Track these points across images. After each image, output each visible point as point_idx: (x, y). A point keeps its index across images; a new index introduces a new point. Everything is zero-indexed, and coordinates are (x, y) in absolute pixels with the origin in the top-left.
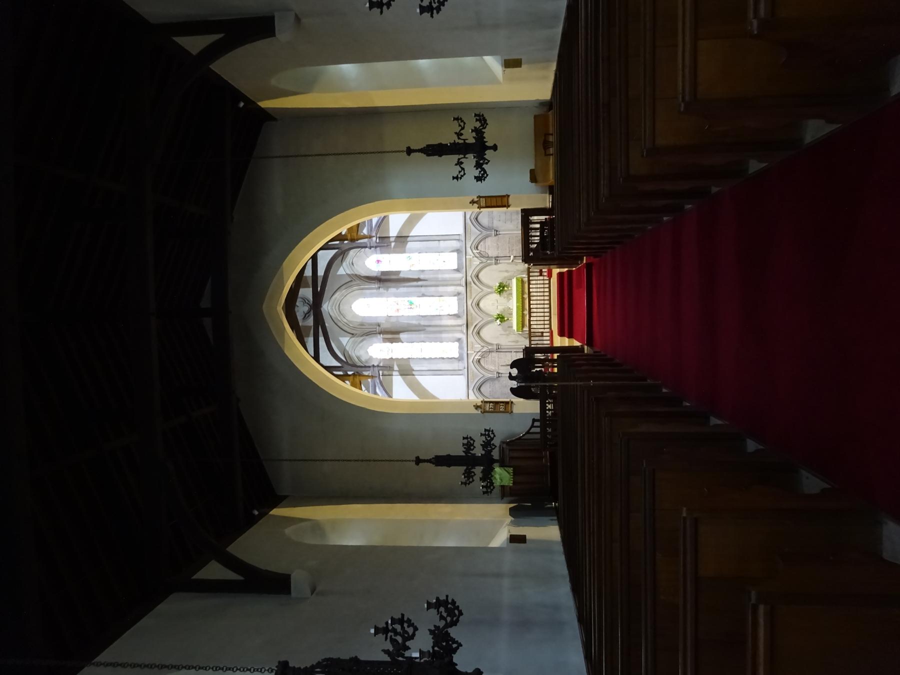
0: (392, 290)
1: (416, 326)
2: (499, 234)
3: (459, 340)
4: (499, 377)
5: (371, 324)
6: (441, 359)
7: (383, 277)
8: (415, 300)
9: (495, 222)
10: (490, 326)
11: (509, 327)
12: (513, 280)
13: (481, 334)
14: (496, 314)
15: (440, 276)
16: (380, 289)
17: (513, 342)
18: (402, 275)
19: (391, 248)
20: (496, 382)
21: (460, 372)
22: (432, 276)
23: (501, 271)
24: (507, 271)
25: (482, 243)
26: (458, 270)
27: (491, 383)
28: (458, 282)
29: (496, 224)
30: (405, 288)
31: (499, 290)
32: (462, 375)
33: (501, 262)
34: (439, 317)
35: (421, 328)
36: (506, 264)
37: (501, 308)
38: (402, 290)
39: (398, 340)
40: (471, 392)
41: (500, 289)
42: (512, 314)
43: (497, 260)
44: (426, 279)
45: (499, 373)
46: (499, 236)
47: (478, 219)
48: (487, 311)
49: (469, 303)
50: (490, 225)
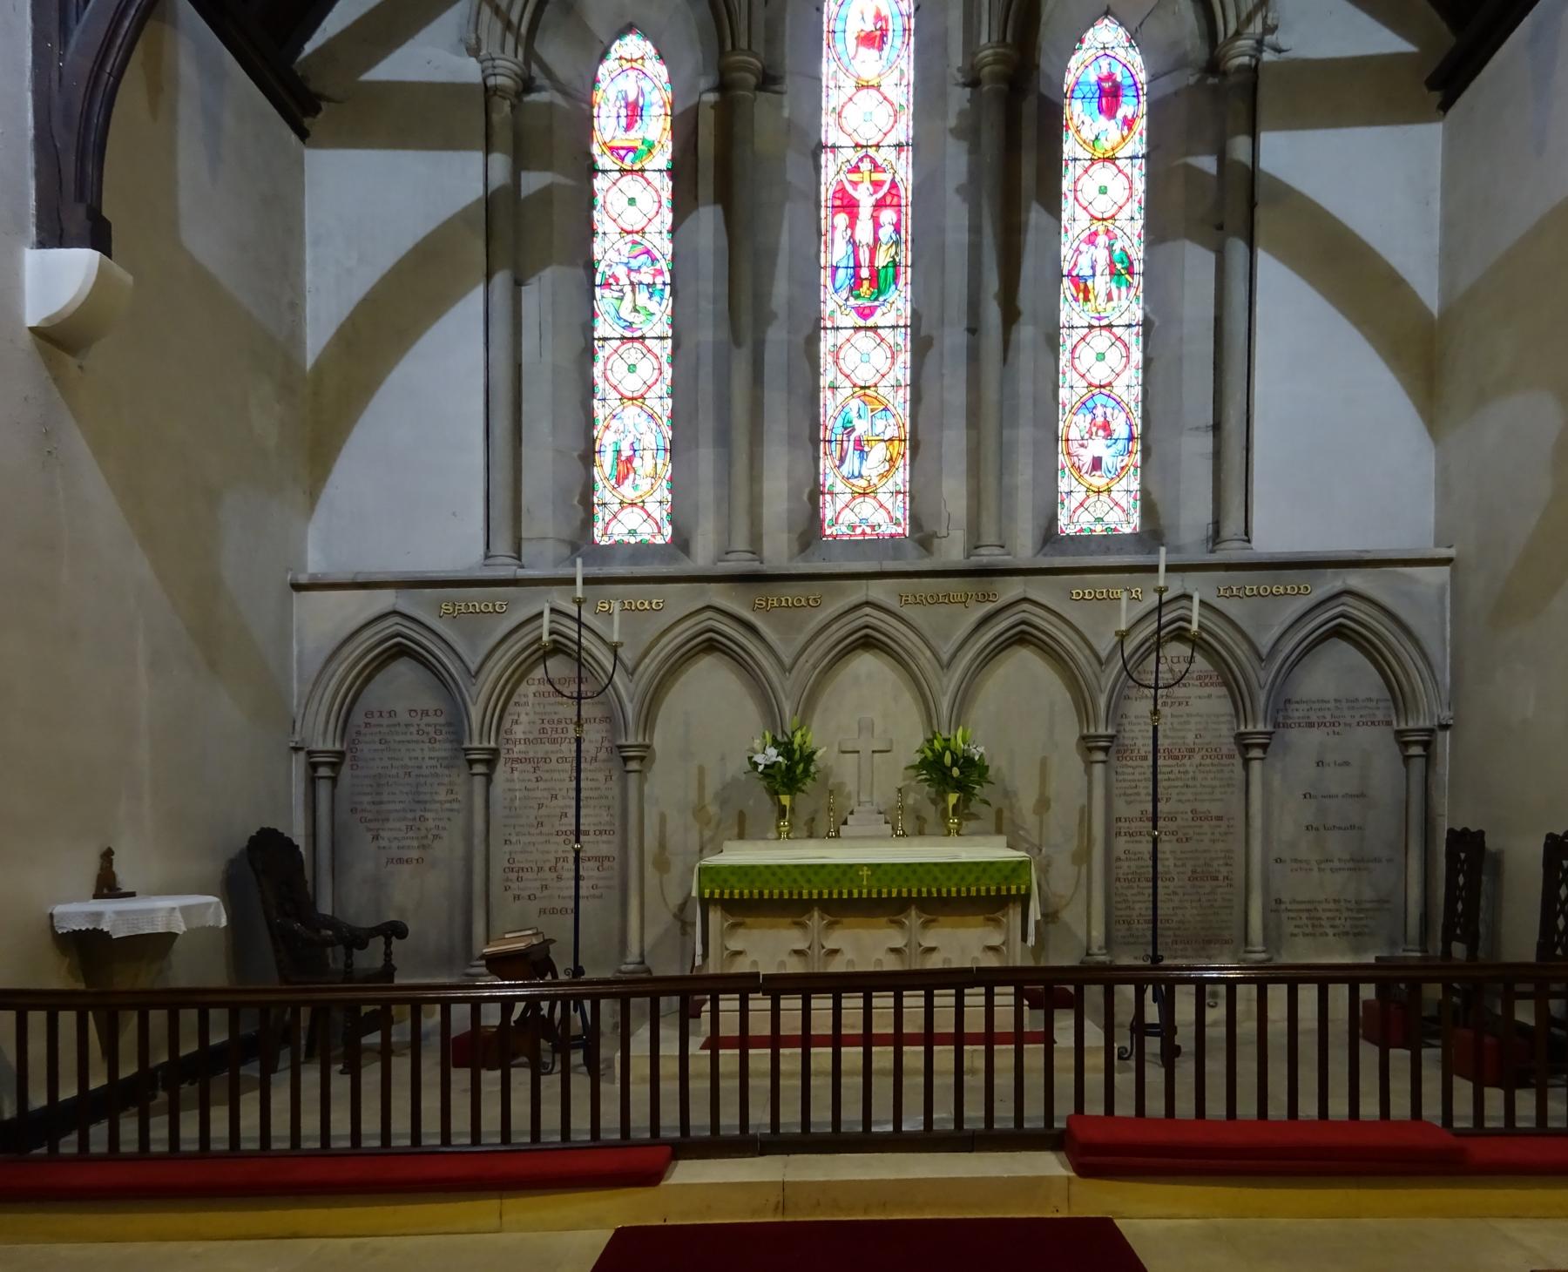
0: (956, 161)
1: (761, 298)
2: (1246, 763)
3: (681, 542)
4: (471, 763)
5: (773, 36)
6: (581, 446)
7: (1029, 107)
8: (897, 305)
9: (1316, 736)
10: (751, 709)
11: (742, 818)
12: (1003, 839)
13: (707, 663)
14: (812, 740)
15: (1024, 434)
16: (968, 90)
17: (662, 845)
18: (1035, 216)
19: (1189, 153)
20: (442, 749)
21: (502, 545)
22: (1025, 387)
23: (1044, 764)
24: (1043, 804)
25: (1201, 663)
26: (1049, 535)
27: (442, 720)
28: (989, 536)
29: (1305, 741)
30: (964, 237)
31: (948, 759)
32: (487, 557)
33: (1098, 770)
34: (806, 433)
35: (746, 319)
36: (1084, 801)
37: (846, 771)
38: (956, 217)
39: (683, 204)
40: (385, 600)
41: (955, 763)
42: (811, 836)
43: (1106, 750)
44: (1011, 354)
45: (491, 764)
46: (1238, 761)
47: (1335, 640)
48: (826, 699)
49: (877, 591)
50: (1297, 713)
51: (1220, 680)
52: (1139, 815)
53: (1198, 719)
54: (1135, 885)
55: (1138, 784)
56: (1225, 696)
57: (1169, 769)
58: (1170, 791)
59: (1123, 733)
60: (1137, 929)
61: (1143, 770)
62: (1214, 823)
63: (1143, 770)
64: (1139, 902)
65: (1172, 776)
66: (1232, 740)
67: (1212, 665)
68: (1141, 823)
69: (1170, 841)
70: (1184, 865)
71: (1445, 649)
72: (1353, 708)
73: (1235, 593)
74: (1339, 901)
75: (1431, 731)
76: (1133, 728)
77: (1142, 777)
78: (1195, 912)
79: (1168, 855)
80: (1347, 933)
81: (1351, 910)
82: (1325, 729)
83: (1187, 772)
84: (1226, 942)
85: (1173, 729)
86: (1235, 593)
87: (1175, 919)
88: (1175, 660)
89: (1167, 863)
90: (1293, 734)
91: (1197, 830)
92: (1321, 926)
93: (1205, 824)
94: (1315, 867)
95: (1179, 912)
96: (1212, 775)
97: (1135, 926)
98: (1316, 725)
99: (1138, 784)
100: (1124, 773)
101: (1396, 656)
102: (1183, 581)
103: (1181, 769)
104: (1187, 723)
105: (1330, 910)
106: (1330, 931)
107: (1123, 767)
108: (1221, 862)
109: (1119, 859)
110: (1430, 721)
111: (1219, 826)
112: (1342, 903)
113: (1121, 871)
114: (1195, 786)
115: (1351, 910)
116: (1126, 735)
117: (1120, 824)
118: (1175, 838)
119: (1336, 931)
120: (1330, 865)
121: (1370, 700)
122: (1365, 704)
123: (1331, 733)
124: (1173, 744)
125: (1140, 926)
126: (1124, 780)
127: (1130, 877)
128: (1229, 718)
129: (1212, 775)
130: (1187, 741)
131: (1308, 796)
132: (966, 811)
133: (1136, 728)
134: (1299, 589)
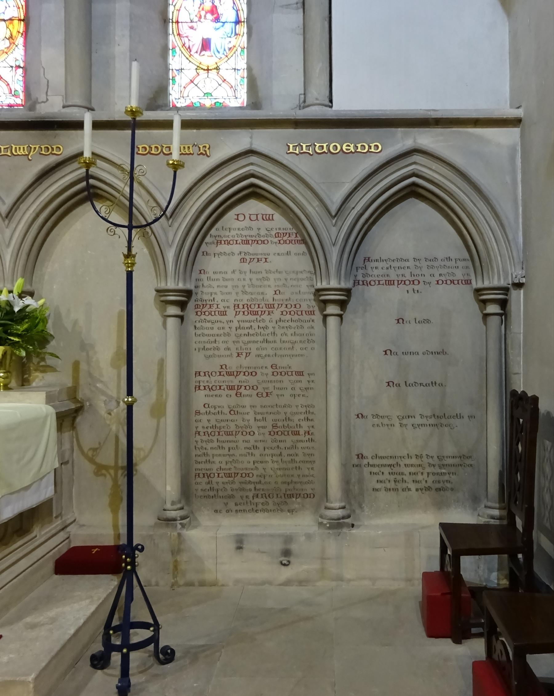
2: (325, 317)
46: (318, 317)
51: (299, 238)
52: (218, 369)
53: (277, 276)
54: (215, 438)
55: (218, 339)
57: (248, 325)
58: (250, 345)
59: (201, 289)
60: (217, 483)
61: (221, 325)
62: (294, 378)
63: (221, 325)
64: (220, 455)
65: (251, 332)
66: (312, 297)
67: (292, 226)
68: (221, 378)
69: (251, 396)
70: (264, 419)
71: (517, 209)
72: (432, 267)
73: (304, 150)
74: (421, 457)
75: (506, 290)
76: (211, 282)
77: (222, 332)
78: (276, 466)
79: (248, 409)
80: (429, 489)
81: (434, 466)
82: (406, 288)
83: (266, 327)
85: (253, 286)
86: (304, 150)
87: (255, 473)
88: (253, 217)
89: (247, 417)
90: (373, 291)
91: (278, 385)
92: (403, 481)
93: (286, 378)
94: (397, 423)
95: (259, 466)
96: (292, 331)
97: (215, 479)
98: (396, 283)
99: (218, 339)
100: (202, 328)
101: (469, 216)
102: (251, 138)
103: (262, 325)
104: (268, 279)
105: (412, 465)
106: (413, 486)
107: (201, 321)
108: (302, 417)
109: (198, 413)
110: (505, 280)
111: (300, 381)
113: (200, 425)
114: (275, 342)
115: (434, 466)
116: (205, 290)
117: (199, 378)
118: (255, 392)
119: (419, 486)
120: (411, 421)
121: (449, 259)
122: (443, 263)
123: (411, 292)
124: (252, 300)
125: (220, 480)
126: (203, 335)
127: (210, 430)
128: (309, 275)
129: (292, 331)
130: (266, 297)
131: (388, 352)
132: (42, 363)
133: (215, 284)
134: (370, 147)
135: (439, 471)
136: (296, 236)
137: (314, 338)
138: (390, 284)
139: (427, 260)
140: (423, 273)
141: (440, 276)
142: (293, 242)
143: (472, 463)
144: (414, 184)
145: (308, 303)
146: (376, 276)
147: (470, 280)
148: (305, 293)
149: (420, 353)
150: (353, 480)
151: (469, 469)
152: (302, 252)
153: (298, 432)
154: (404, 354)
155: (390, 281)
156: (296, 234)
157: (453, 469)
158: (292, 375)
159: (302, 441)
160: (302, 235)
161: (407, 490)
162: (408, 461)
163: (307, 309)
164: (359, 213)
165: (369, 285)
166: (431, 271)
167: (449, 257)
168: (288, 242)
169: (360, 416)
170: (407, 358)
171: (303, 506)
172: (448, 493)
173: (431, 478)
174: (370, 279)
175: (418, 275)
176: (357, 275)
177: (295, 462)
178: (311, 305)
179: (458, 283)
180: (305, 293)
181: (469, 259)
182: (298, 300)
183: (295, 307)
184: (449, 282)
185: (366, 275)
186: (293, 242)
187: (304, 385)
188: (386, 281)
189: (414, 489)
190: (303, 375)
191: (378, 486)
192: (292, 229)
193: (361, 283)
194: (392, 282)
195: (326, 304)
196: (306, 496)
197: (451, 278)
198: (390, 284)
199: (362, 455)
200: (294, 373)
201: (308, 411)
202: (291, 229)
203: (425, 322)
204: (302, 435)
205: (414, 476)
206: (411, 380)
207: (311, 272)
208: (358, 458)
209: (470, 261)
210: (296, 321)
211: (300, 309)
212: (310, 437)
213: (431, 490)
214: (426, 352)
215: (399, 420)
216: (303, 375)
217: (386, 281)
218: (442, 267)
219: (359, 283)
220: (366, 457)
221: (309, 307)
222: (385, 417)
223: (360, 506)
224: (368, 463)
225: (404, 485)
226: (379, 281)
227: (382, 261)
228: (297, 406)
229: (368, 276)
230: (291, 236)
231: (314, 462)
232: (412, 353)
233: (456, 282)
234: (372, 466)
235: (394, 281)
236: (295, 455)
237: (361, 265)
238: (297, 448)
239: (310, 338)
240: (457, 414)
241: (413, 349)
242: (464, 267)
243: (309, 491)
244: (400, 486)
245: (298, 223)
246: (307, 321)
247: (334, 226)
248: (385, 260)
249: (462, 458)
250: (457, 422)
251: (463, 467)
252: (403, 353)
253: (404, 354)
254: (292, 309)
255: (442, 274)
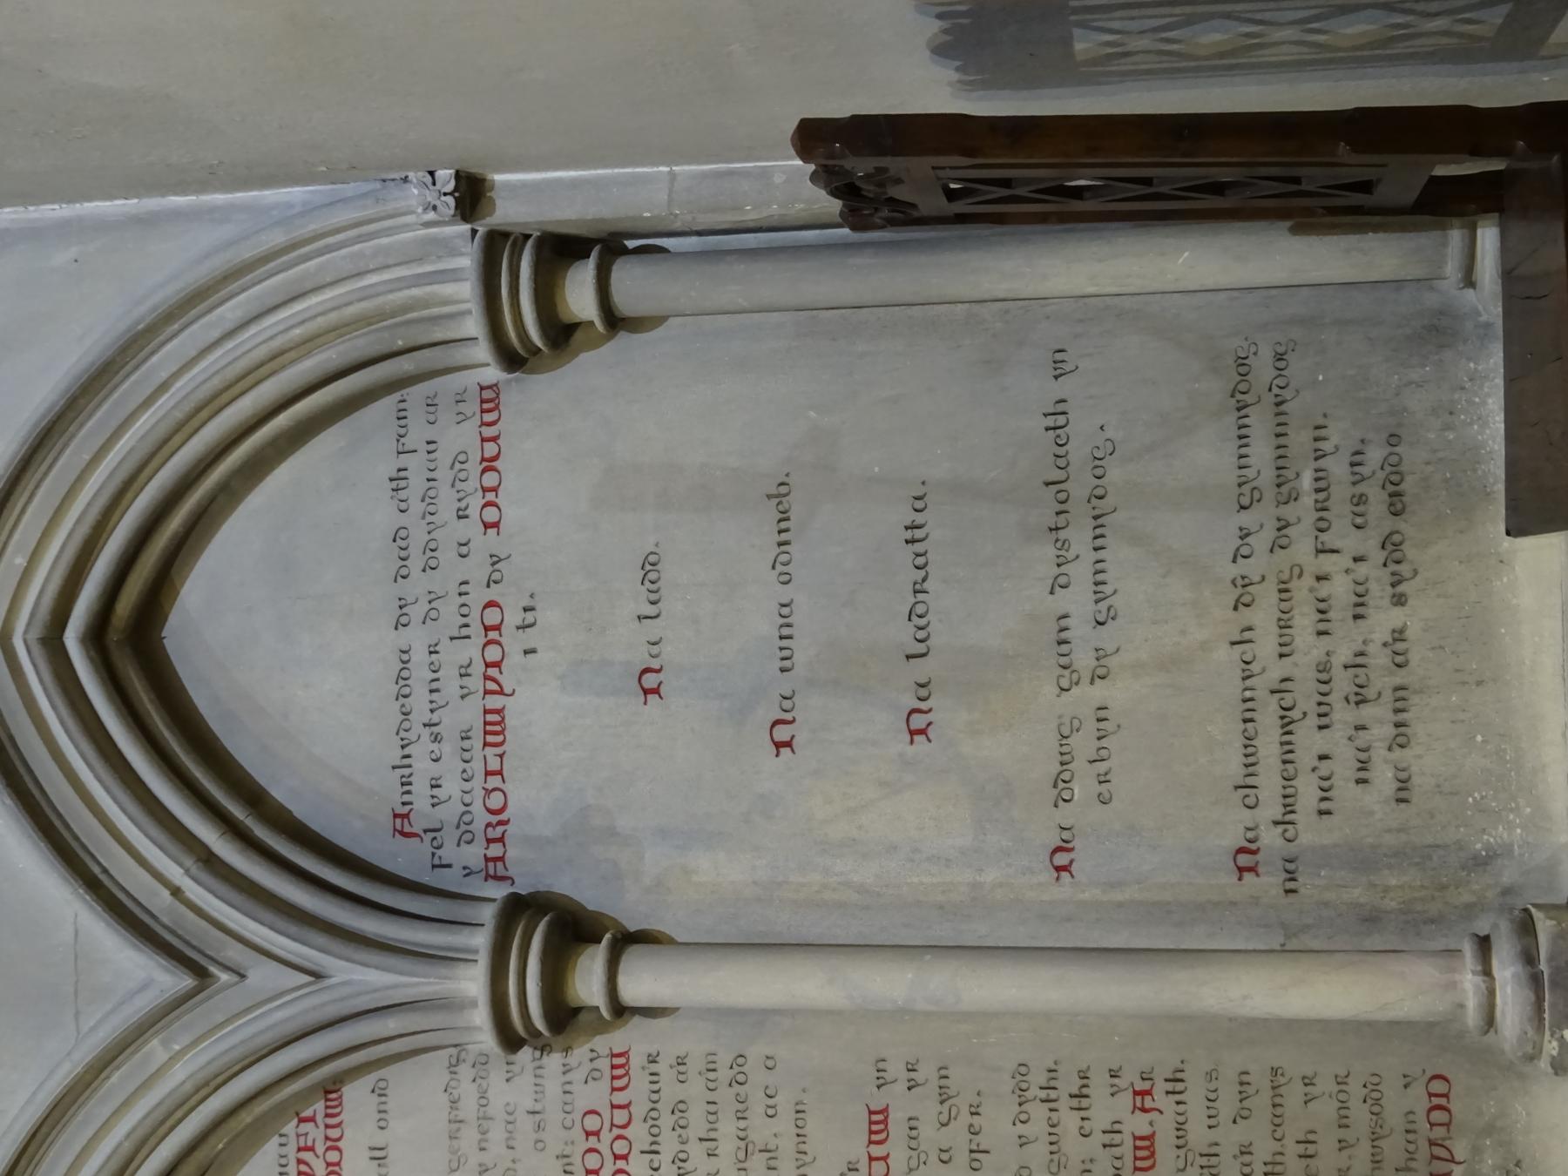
46: (633, 1038)
51: (319, 1107)
56: (380, 1092)
66: (554, 1061)
72: (431, 549)
82: (514, 658)
84: (1439, 1104)
96: (696, 1151)
98: (494, 702)
105: (1284, 625)
108: (1070, 1121)
111: (912, 1125)
112: (1252, 568)
119: (1379, 592)
120: (1079, 629)
121: (398, 479)
122: (417, 507)
123: (530, 638)
128: (465, 1071)
129: (696, 1151)
135: (1308, 500)
136: (312, 1119)
137: (724, 1058)
138: (498, 728)
139: (404, 572)
140: (453, 588)
141: (467, 517)
142: (334, 1133)
143: (1266, 354)
144: (96, 636)
145: (578, 1076)
146: (467, 786)
147: (482, 388)
148: (539, 1091)
149: (786, 594)
150: (1357, 894)
151: (1297, 367)
152: (375, 1099)
153: (1139, 1143)
154: (787, 664)
155: (489, 728)
156: (302, 1120)
157: (1300, 440)
158: (885, 1158)
159: (1180, 1127)
160: (305, 1096)
161: (1400, 646)
162: (1266, 645)
163: (605, 1085)
164: (194, 870)
165: (503, 817)
166: (447, 555)
167: (391, 480)
168: (333, 1156)
169: (1061, 859)
170: (803, 654)
171: (1490, 1130)
172: (1413, 458)
173: (1343, 536)
174: (477, 808)
175: (465, 610)
176: (464, 868)
177: (1279, 1158)
178: (587, 1066)
179: (494, 439)
180: (539, 1091)
181: (397, 396)
182: (568, 1124)
183: (597, 1134)
184: (490, 479)
185: (463, 828)
186: (334, 1133)
187: (928, 1110)
188: (486, 744)
189: (1396, 616)
190: (885, 1111)
191: (1383, 777)
192: (281, 1135)
193: (495, 850)
194: (490, 718)
195: (574, 1005)
196: (1437, 1116)
197: (474, 467)
198: (498, 728)
199: (1241, 850)
200: (877, 1151)
201: (1043, 1094)
202: (283, 1140)
203: (652, 576)
204: (1151, 1124)
205: (1331, 615)
206: (904, 634)
207: (454, 1061)
208: (1252, 869)
209: (404, 392)
210: (655, 1131)
211: (606, 1114)
212: (1160, 1087)
213: (1396, 538)
214: (779, 568)
215: (1077, 683)
216: (885, 1111)
217: (486, 744)
218: (432, 509)
219: (496, 860)
220: (1250, 835)
221: (596, 1074)
222: (1065, 749)
223: (1482, 862)
224: (1276, 823)
225: (1379, 659)
226: (488, 773)
227: (406, 761)
228: (1023, 1142)
229: (467, 818)
230: (310, 1143)
231: (1275, 1071)
232: (785, 631)
233: (491, 450)
234: (1289, 809)
235: (486, 712)
236: (1247, 1158)
237: (425, 847)
238: (1213, 1150)
239: (724, 1074)
240: (1047, 429)
241: (766, 626)
242: (432, 418)
243: (1417, 1100)
244: (1381, 680)
245: (246, 1117)
246: (655, 1087)
247: (243, 976)
248: (403, 747)
249: (1248, 398)
250: (1081, 428)
251: (1287, 394)
252: (783, 670)
253: (787, 664)
254: (604, 1147)
255: (459, 510)
